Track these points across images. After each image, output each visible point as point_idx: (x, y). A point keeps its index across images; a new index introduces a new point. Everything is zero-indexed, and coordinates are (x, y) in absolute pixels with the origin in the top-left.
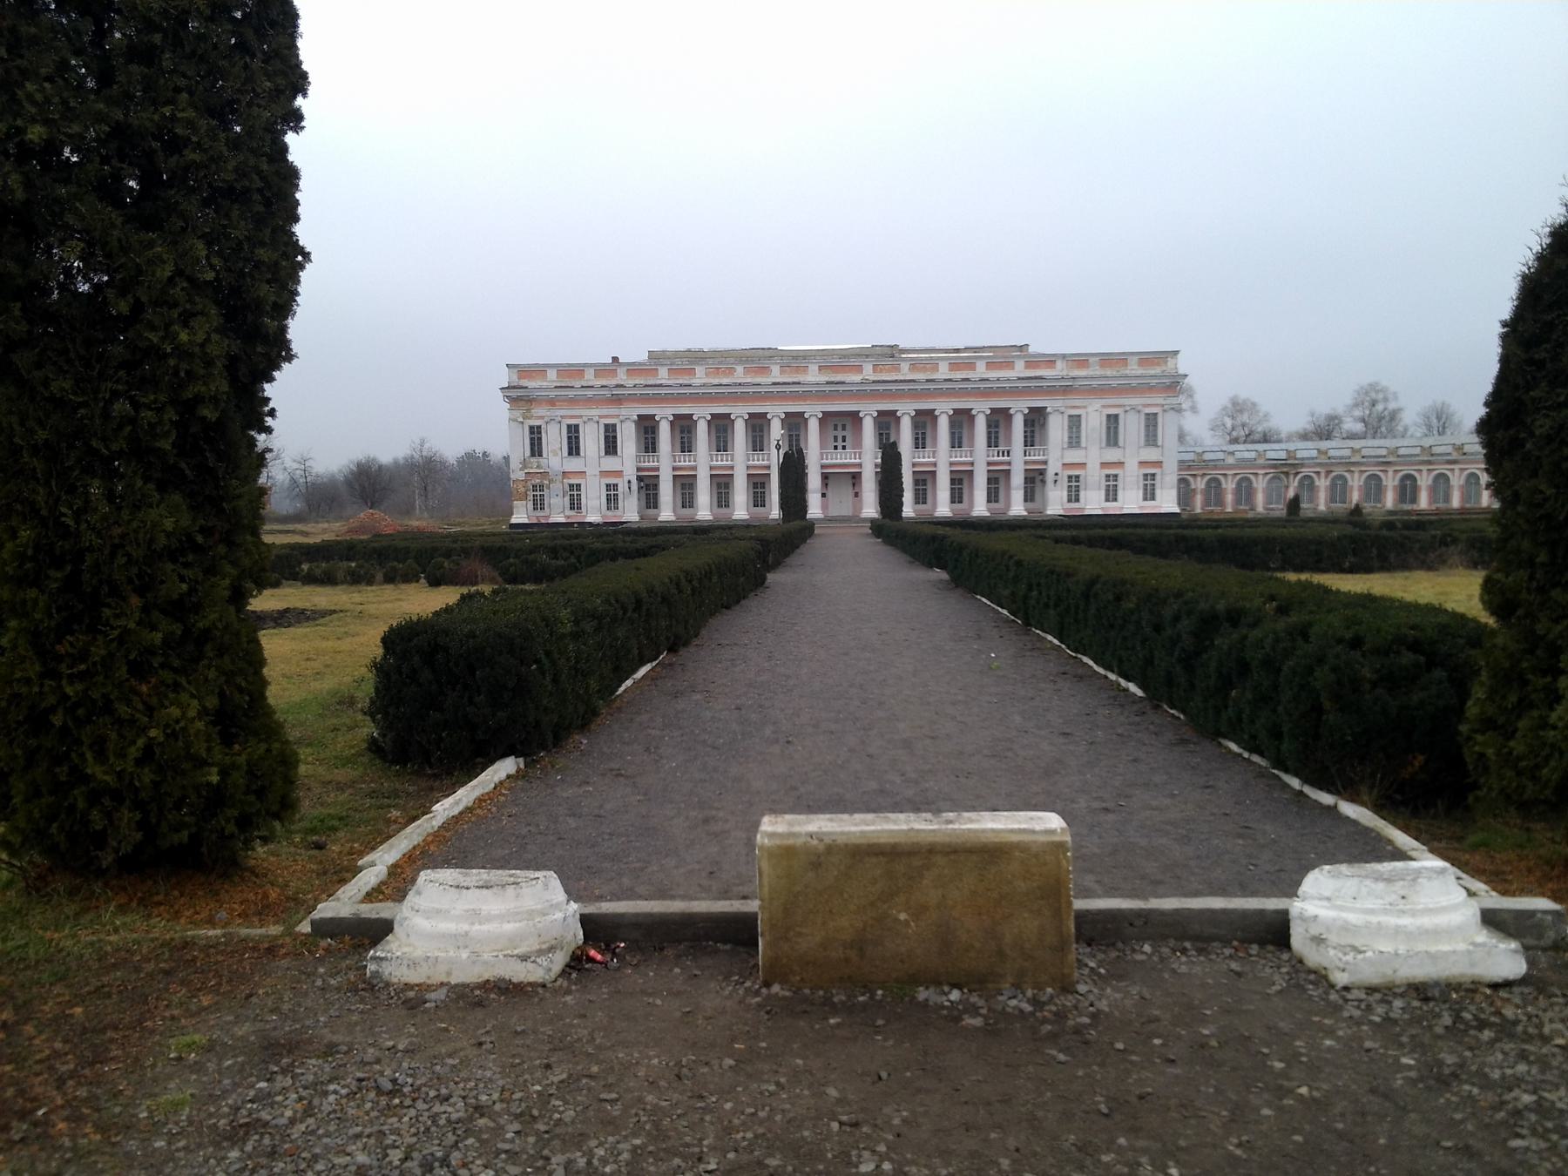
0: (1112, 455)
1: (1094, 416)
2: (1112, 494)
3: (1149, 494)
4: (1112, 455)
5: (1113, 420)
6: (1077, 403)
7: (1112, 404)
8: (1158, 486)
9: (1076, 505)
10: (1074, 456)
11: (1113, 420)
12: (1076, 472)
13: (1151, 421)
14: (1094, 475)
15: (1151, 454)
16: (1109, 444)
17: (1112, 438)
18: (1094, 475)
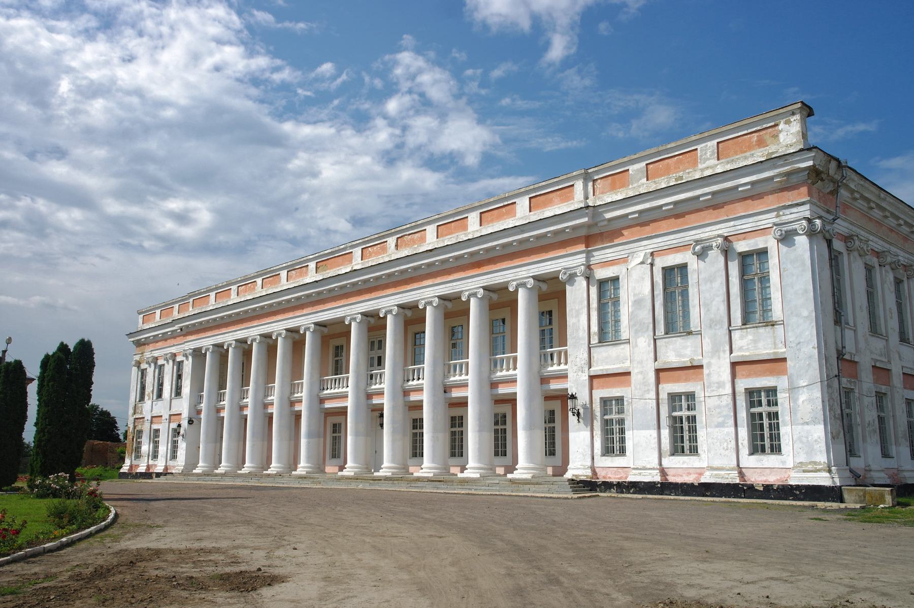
0: (676, 351)
1: (634, 270)
2: (683, 437)
3: (764, 436)
4: (676, 351)
5: (674, 280)
6: (609, 254)
7: (671, 245)
8: (784, 418)
9: (618, 461)
10: (608, 359)
11: (674, 280)
12: (615, 392)
13: (751, 267)
14: (641, 399)
15: (752, 343)
16: (670, 329)
17: (673, 313)
18: (641, 399)
